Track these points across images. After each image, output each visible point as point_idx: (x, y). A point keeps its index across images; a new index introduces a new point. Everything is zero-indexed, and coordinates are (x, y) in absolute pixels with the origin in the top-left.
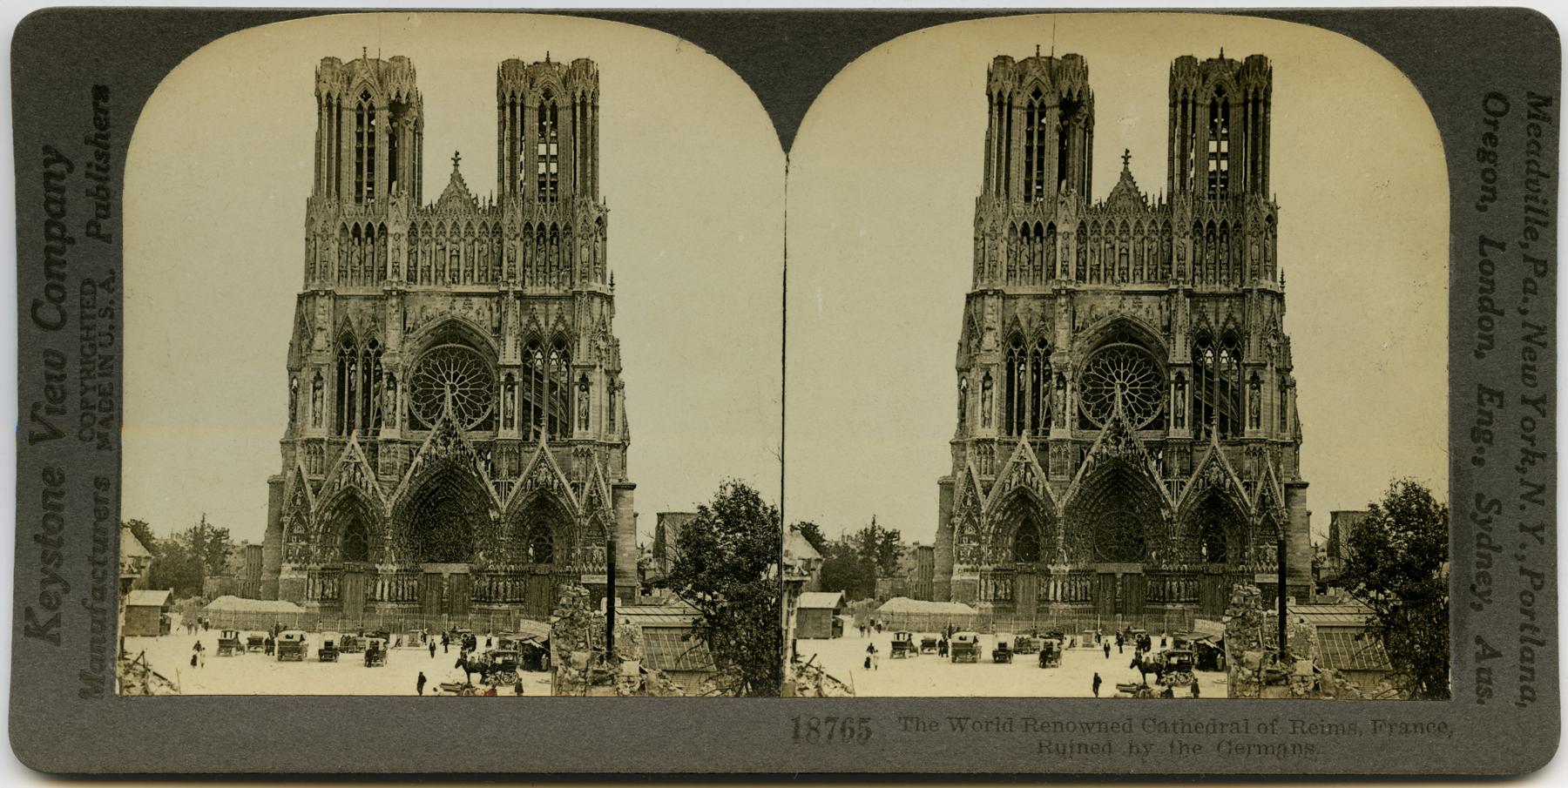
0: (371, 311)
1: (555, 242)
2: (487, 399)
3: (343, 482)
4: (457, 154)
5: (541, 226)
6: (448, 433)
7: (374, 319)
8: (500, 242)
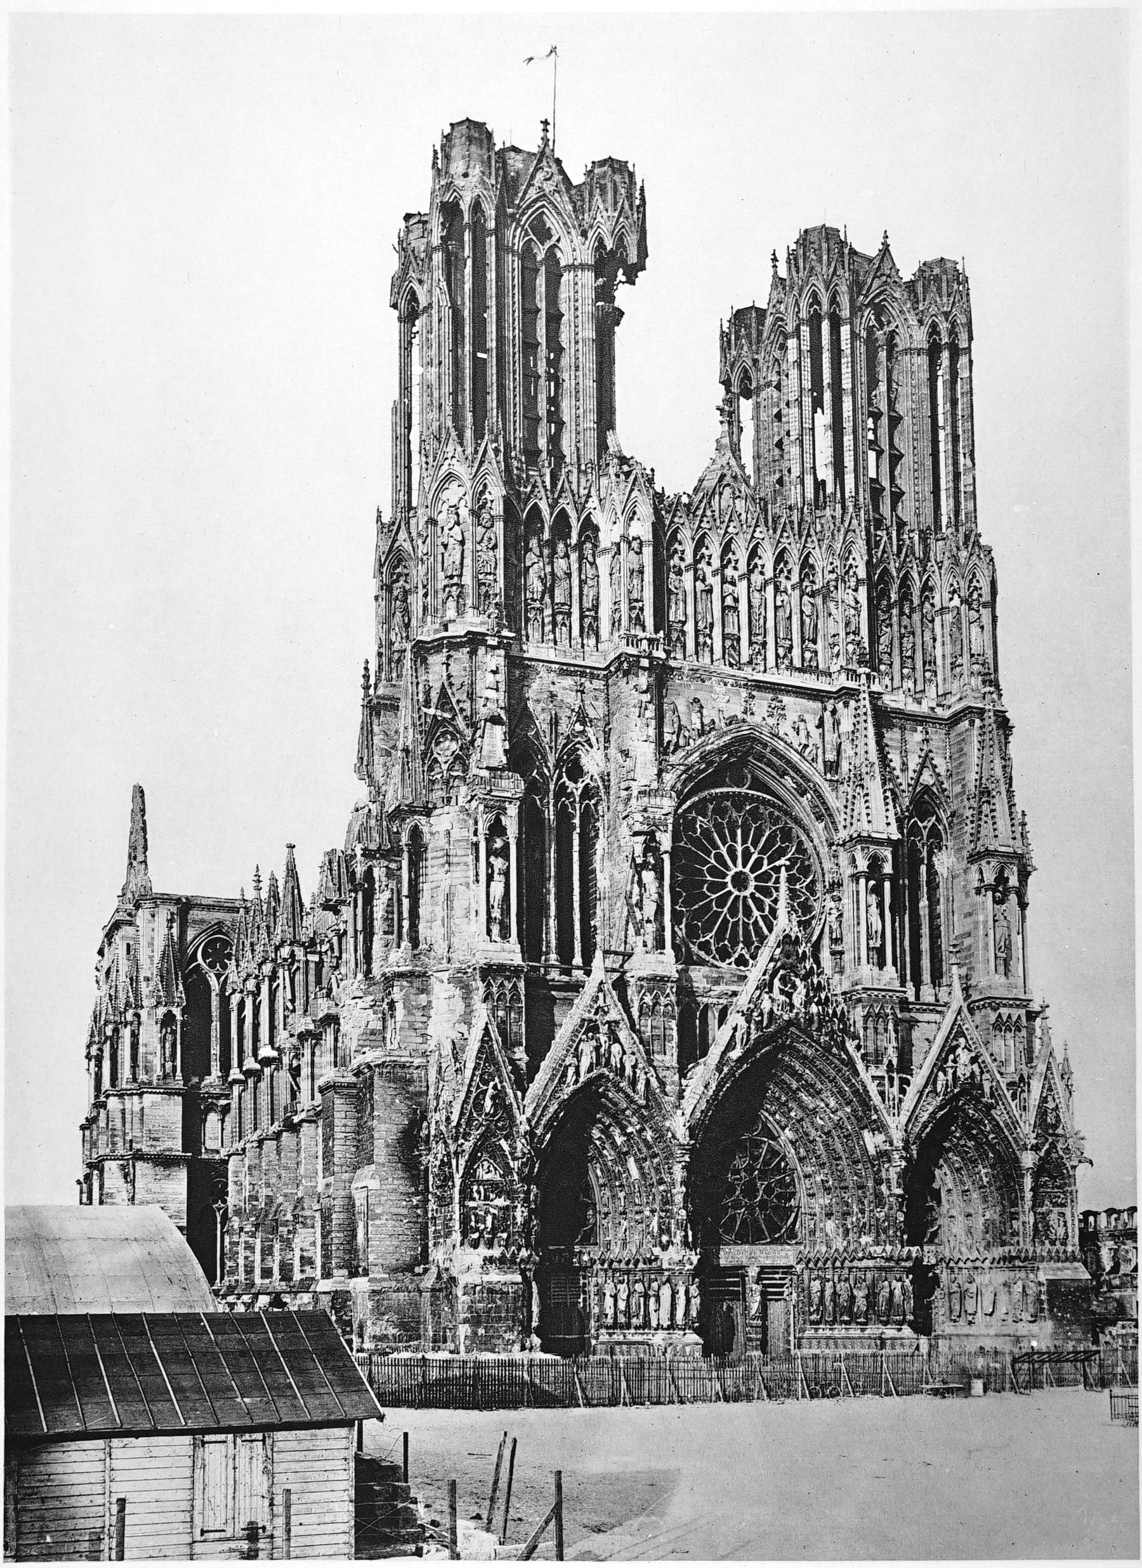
0: (572, 699)
3: (585, 1063)
7: (582, 717)
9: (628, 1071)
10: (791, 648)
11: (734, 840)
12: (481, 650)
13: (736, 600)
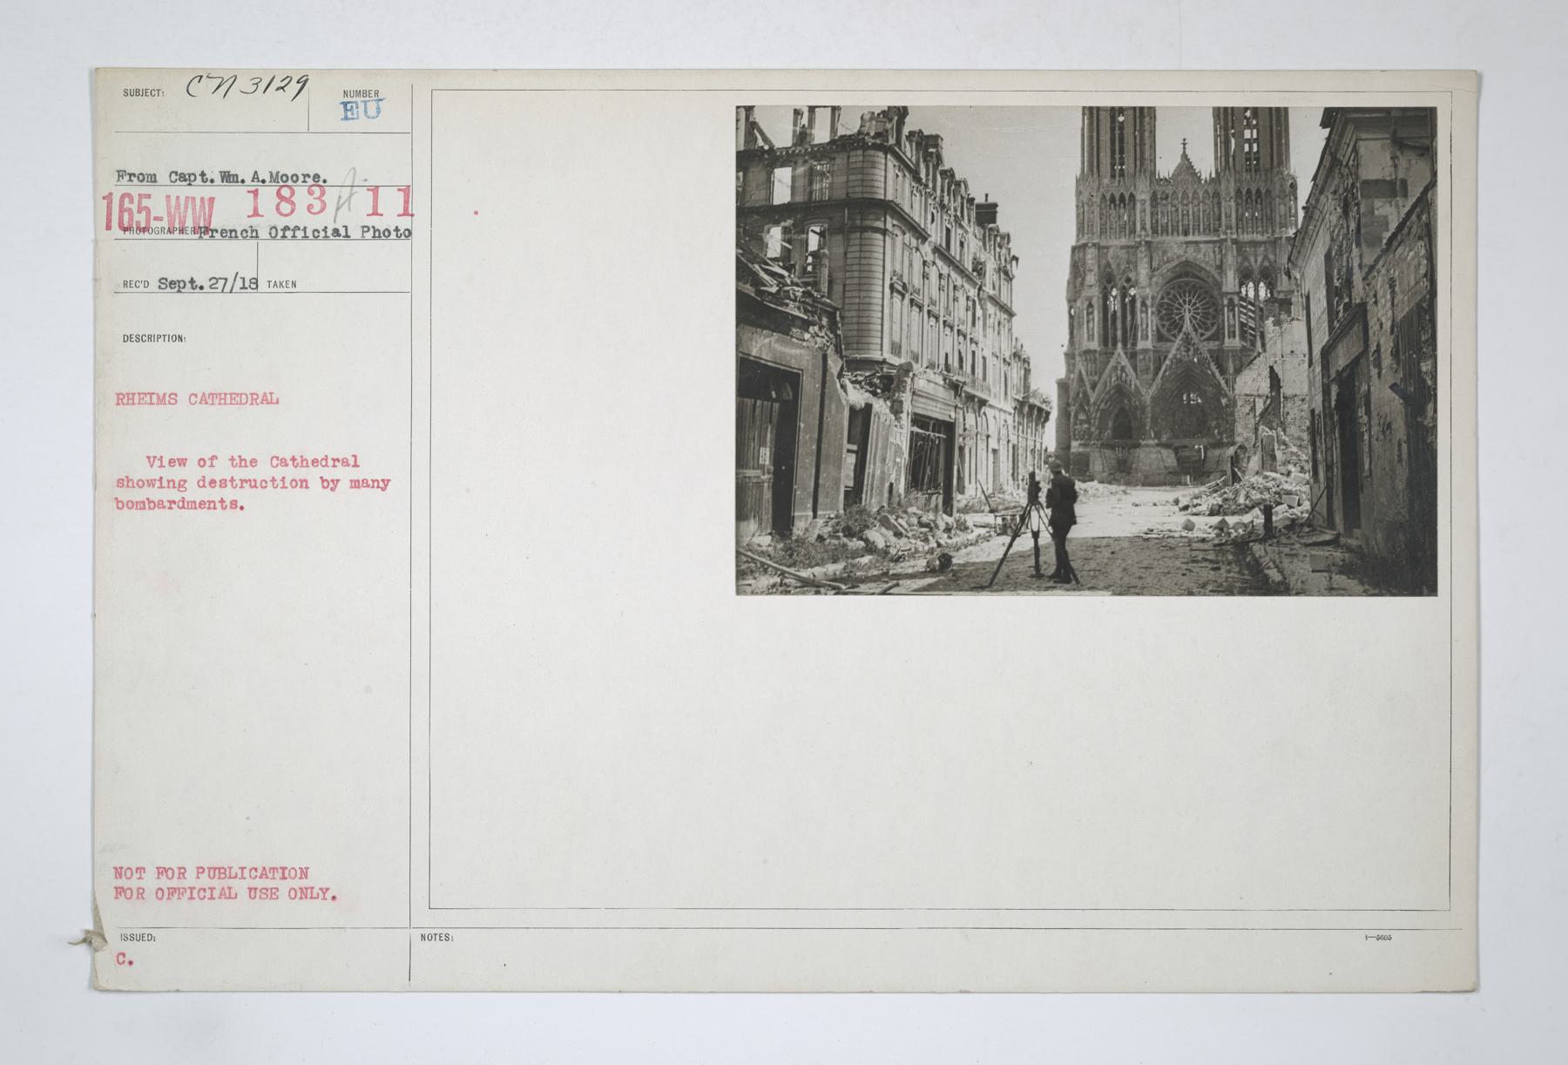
1: (1259, 202)
2: (1214, 317)
3: (1113, 380)
4: (1185, 140)
5: (1249, 191)
6: (1187, 341)
8: (1219, 203)
9: (1128, 382)
11: (1185, 296)
13: (1188, 212)
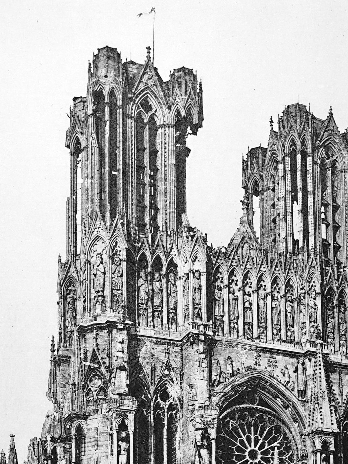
7: (168, 367)
10: (280, 330)
11: (250, 432)
12: (114, 331)
13: (251, 304)
